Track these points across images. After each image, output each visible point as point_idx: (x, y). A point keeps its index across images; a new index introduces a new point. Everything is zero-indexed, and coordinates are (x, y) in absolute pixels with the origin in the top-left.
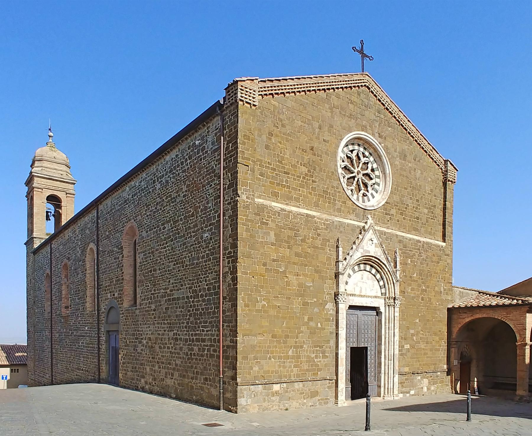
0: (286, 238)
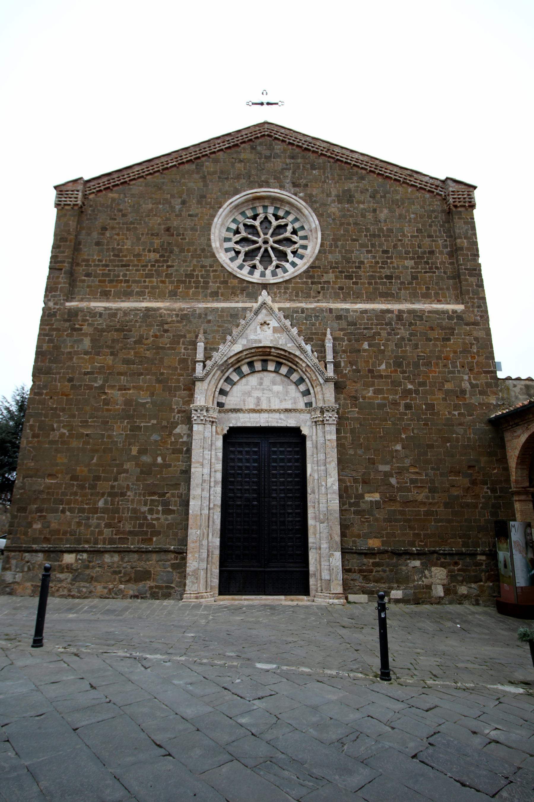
0: (109, 343)
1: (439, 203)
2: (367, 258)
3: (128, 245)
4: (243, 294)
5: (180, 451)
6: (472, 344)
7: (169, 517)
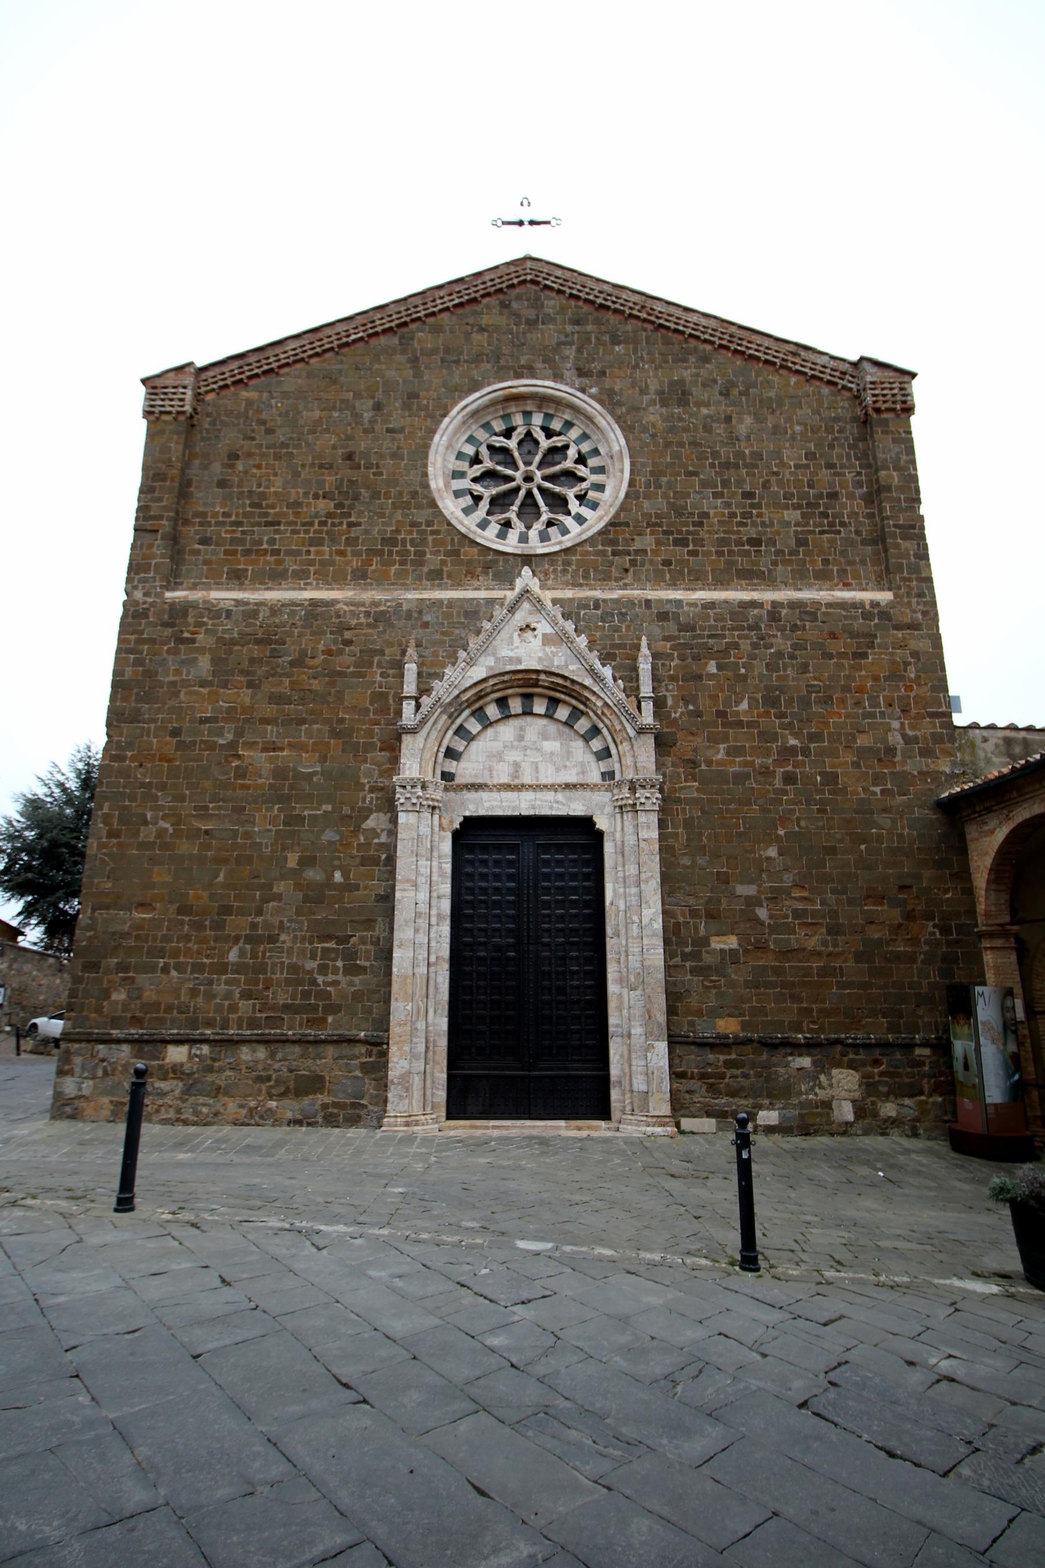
0: (245, 664)
1: (846, 405)
2: (715, 508)
3: (277, 485)
4: (487, 574)
5: (375, 861)
6: (907, 664)
7: (356, 980)
